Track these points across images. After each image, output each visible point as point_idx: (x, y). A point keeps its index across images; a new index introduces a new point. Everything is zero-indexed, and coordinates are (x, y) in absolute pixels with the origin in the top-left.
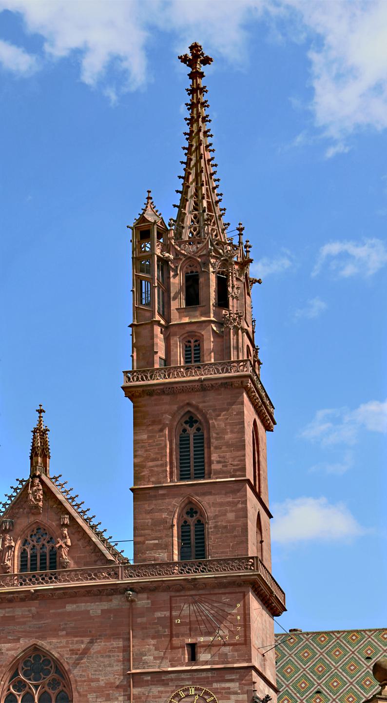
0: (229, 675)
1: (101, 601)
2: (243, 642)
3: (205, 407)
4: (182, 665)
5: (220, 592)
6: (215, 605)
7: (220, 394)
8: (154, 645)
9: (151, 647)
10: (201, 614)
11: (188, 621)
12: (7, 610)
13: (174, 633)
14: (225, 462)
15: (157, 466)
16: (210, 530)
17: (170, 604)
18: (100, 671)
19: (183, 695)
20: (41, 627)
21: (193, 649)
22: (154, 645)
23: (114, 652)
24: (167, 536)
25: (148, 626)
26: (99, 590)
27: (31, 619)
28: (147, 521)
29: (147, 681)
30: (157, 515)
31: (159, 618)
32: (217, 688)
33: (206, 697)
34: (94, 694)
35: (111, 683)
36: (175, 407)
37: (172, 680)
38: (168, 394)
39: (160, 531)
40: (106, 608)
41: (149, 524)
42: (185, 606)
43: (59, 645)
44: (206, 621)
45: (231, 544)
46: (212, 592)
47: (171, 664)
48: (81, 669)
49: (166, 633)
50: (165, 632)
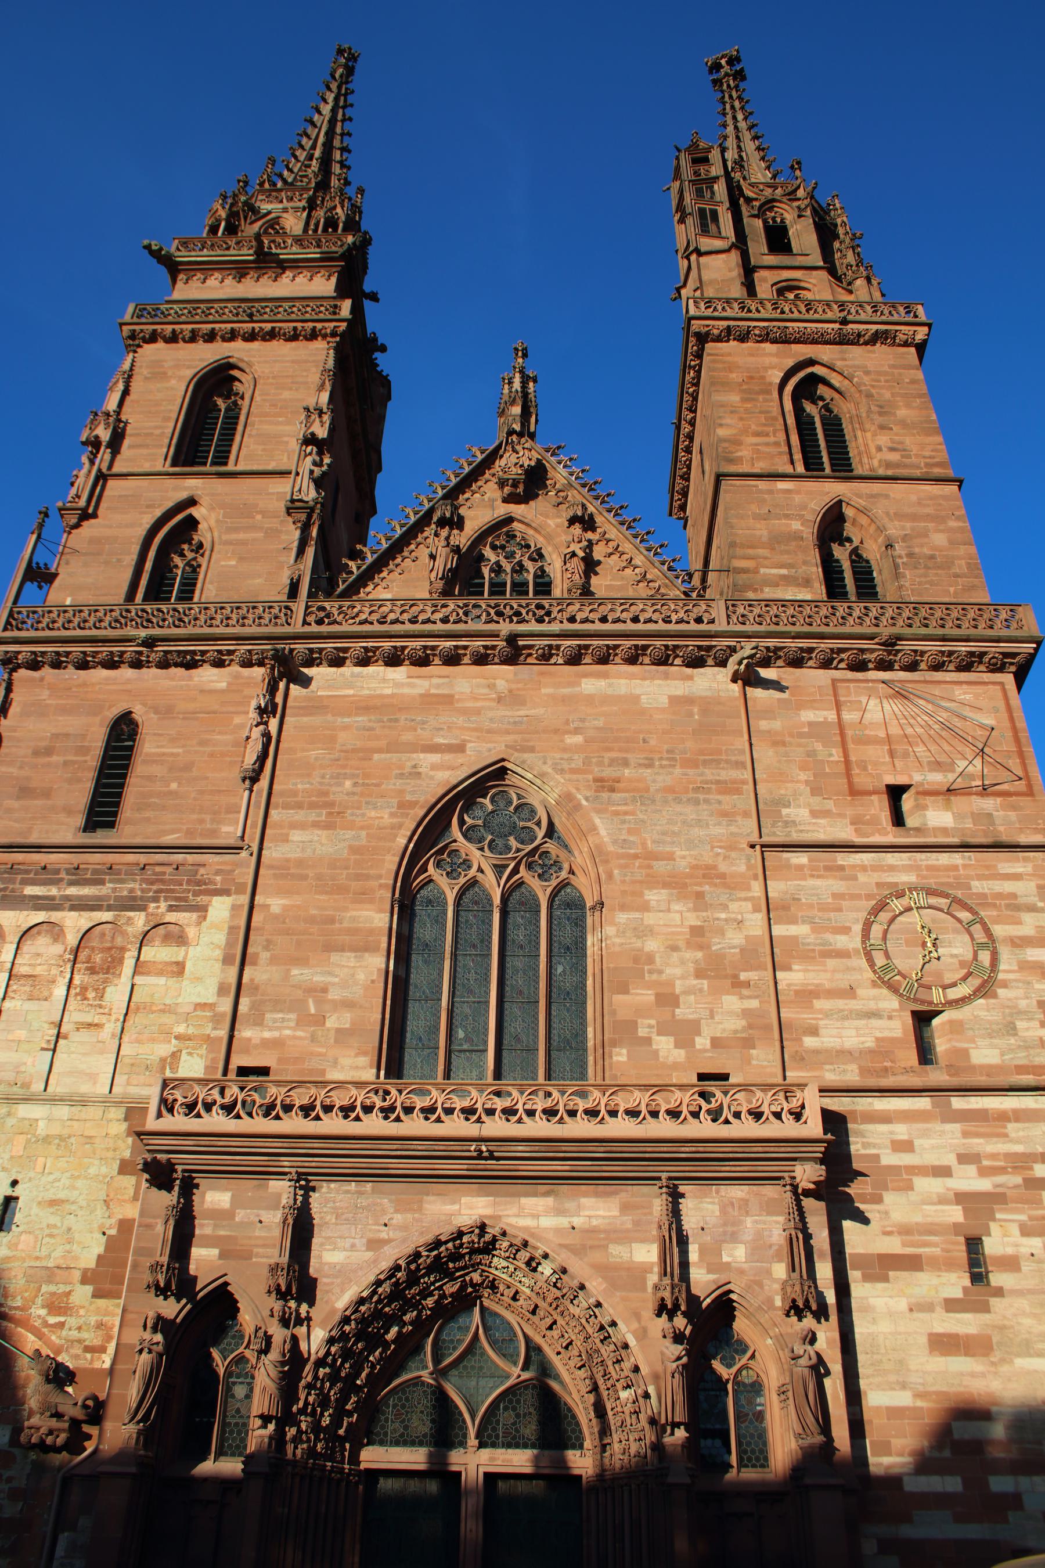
0: (1006, 865)
1: (666, 677)
3: (847, 366)
4: (883, 832)
5: (948, 679)
6: (943, 704)
7: (874, 352)
8: (807, 782)
9: (802, 787)
10: (912, 721)
11: (882, 734)
12: (435, 681)
13: (853, 758)
14: (905, 450)
15: (767, 444)
17: (835, 695)
18: (674, 833)
20: (521, 723)
22: (807, 782)
23: (709, 791)
24: (805, 563)
25: (787, 739)
27: (494, 704)
28: (758, 533)
29: (800, 868)
30: (780, 524)
31: (811, 724)
34: (663, 891)
35: (708, 867)
36: (790, 363)
38: (774, 341)
39: (788, 552)
40: (679, 692)
41: (764, 539)
42: (872, 703)
43: (566, 766)
44: (925, 737)
45: (952, 589)
47: (856, 830)
48: (626, 826)
49: (832, 759)
50: (831, 755)
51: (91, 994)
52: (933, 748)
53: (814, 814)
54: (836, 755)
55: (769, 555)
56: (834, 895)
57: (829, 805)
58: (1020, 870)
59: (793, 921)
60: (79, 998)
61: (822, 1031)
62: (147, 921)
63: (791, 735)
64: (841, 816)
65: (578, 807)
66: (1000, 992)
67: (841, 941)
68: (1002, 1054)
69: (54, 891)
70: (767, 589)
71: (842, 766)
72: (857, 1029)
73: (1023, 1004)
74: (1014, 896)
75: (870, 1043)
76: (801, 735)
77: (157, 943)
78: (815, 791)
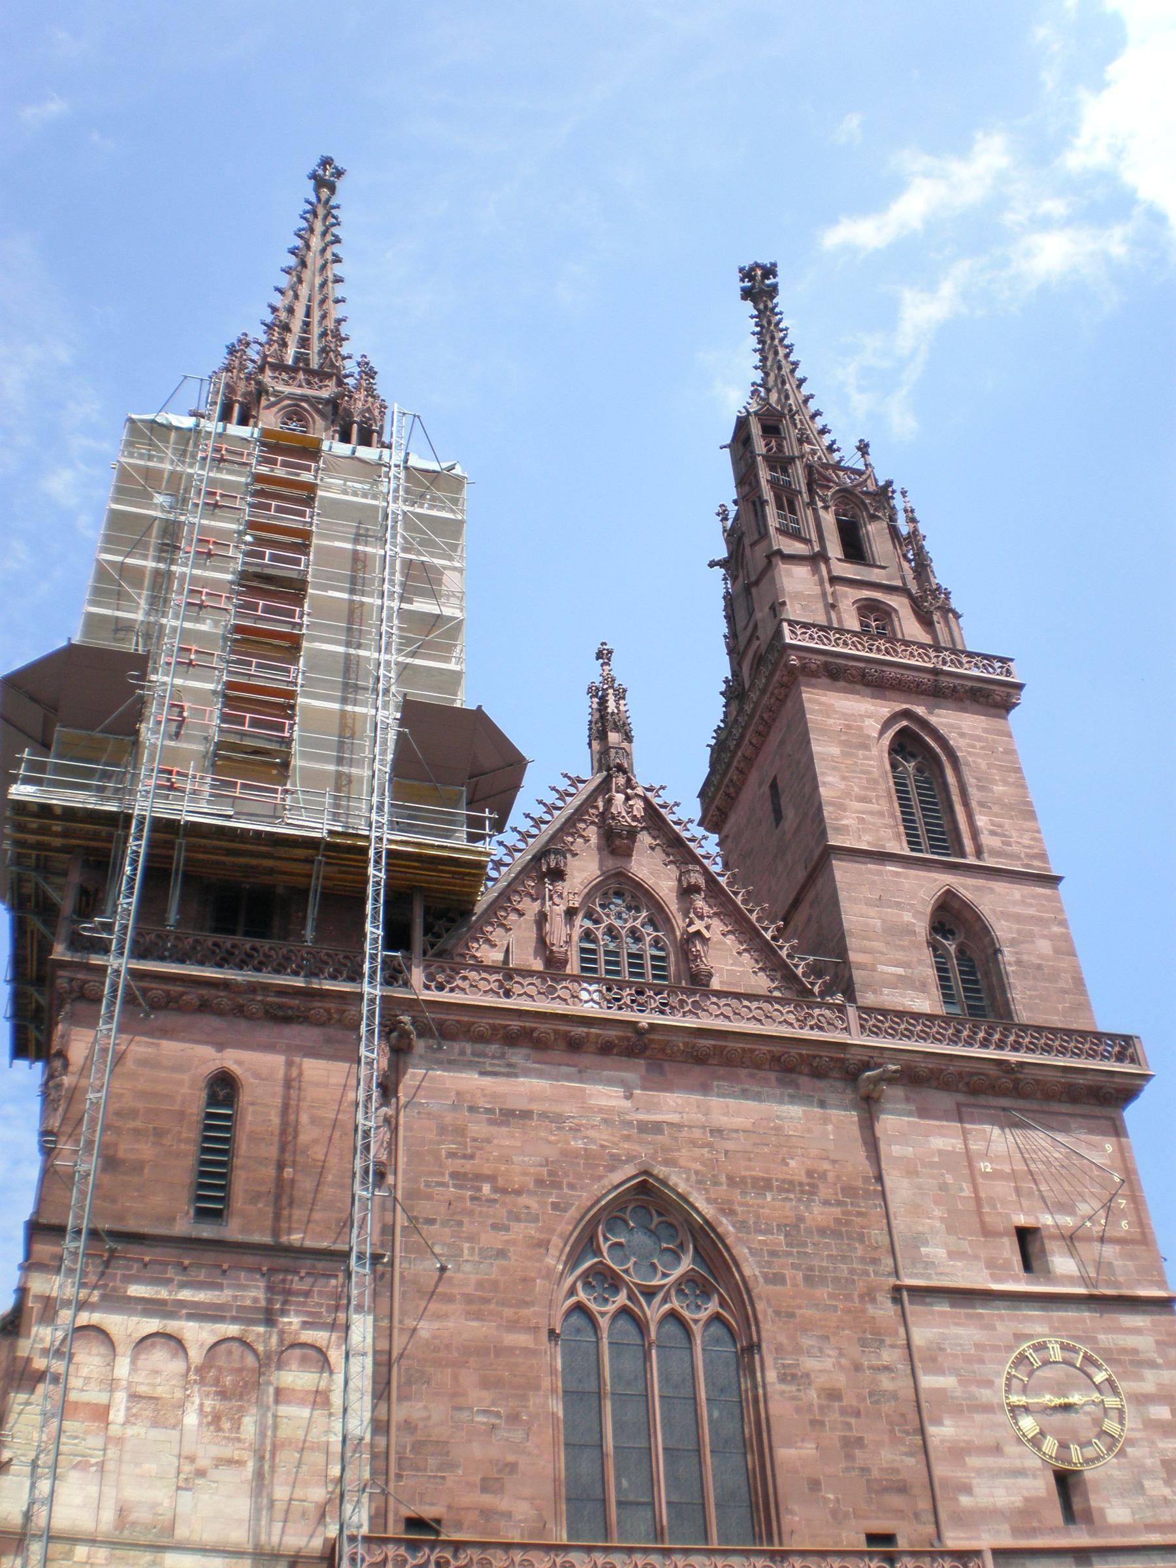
2: (1138, 1237)
8: (942, 1219)
9: (938, 1224)
13: (983, 1195)
15: (871, 813)
16: (1009, 969)
19: (1036, 1358)
21: (1025, 1236)
22: (942, 1219)
26: (800, 1055)
29: (941, 1314)
31: (941, 1152)
32: (1110, 1350)
33: (1091, 1370)
37: (1001, 1317)
39: (902, 948)
45: (1060, 1007)
46: (1046, 1108)
47: (992, 1275)
49: (963, 1194)
50: (962, 1190)
51: (226, 1425)
52: (1055, 1187)
53: (952, 1255)
54: (967, 1192)
55: (884, 950)
56: (978, 1346)
57: (965, 1246)
58: (1141, 1324)
59: (941, 1371)
60: (212, 1428)
61: (976, 1491)
62: (281, 1341)
63: (924, 1165)
64: (976, 1257)
65: (728, 1233)
66: (1129, 1450)
67: (985, 1395)
68: (1133, 1513)
69: (163, 1293)
70: (886, 991)
71: (972, 1206)
72: (1007, 1488)
73: (1149, 1462)
74: (1135, 1351)
75: (1017, 1501)
76: (932, 1165)
77: (294, 1367)
78: (951, 1229)
